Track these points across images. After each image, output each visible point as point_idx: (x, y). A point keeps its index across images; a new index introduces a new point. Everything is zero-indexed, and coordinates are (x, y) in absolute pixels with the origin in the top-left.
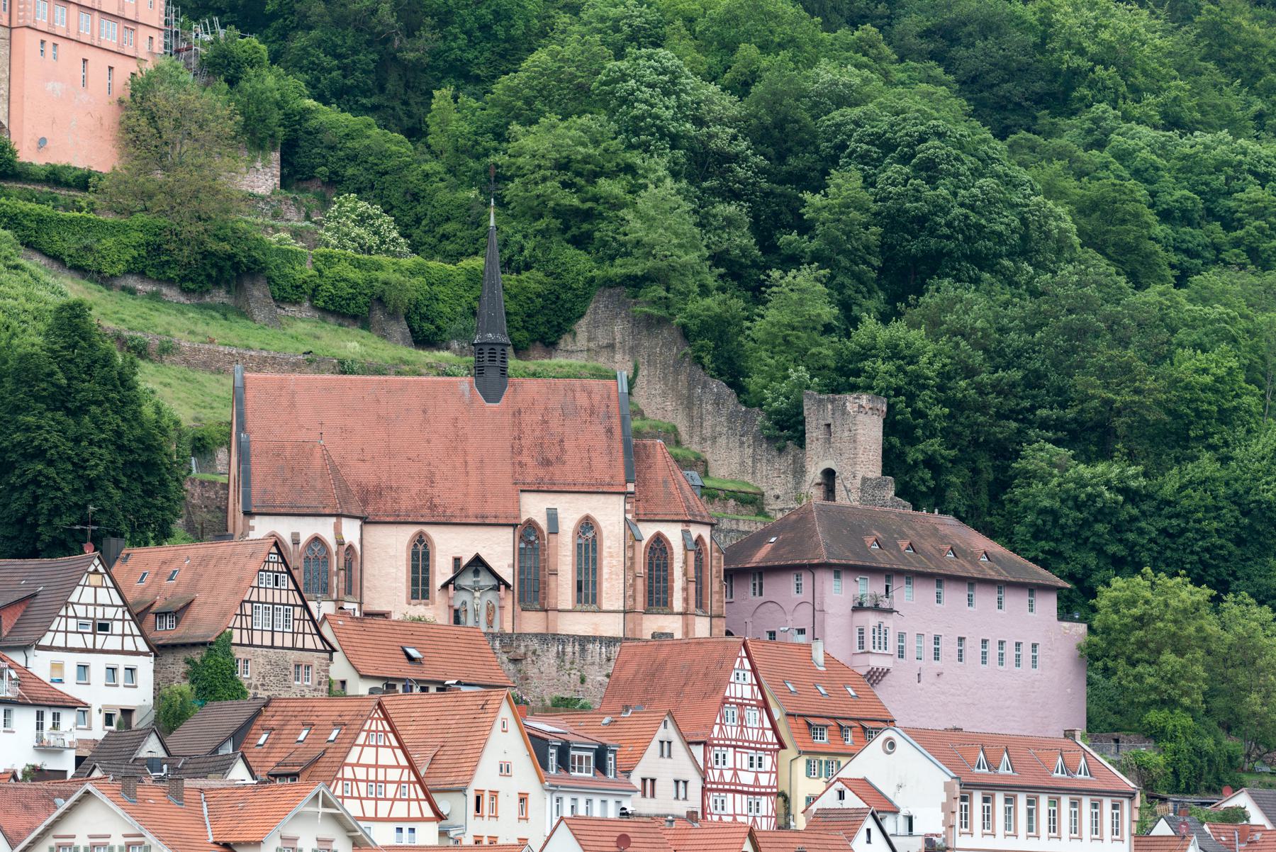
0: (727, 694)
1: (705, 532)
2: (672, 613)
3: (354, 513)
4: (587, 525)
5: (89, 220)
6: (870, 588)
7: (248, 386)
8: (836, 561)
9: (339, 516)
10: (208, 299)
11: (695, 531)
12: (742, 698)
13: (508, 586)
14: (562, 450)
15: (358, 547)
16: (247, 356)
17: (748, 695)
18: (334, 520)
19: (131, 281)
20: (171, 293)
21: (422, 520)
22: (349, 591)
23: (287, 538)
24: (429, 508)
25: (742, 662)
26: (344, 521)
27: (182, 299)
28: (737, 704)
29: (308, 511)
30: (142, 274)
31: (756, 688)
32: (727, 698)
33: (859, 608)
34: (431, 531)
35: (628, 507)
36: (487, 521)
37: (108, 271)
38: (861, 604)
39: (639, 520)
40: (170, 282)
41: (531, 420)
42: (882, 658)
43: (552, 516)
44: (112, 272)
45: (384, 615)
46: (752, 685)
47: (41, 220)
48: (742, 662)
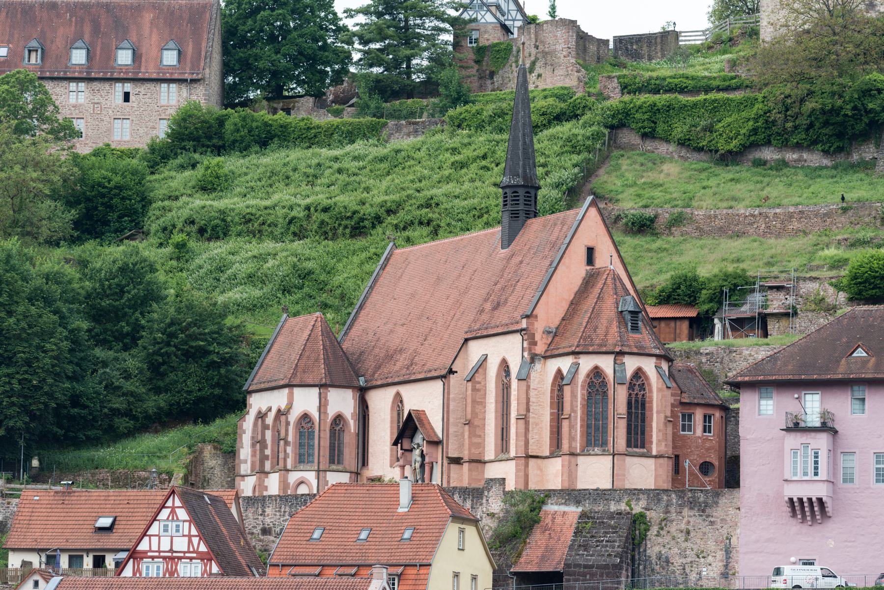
0: (139, 548)
1: (606, 364)
2: (648, 456)
3: (310, 381)
4: (505, 366)
5: (715, 100)
6: (813, 406)
7: (391, 262)
8: (747, 379)
9: (290, 386)
10: (855, 157)
11: (587, 364)
12: (171, 551)
13: (436, 443)
14: (513, 292)
15: (315, 415)
16: (771, 215)
17: (181, 544)
18: (286, 391)
19: (768, 154)
20: (814, 159)
21: (396, 380)
22: (303, 459)
23: (264, 410)
24: (408, 369)
25: (173, 512)
26: (296, 390)
27: (826, 162)
28: (164, 558)
29: (273, 384)
30: (768, 143)
31: (195, 540)
32: (146, 552)
33: (796, 427)
34: (404, 390)
35: (525, 344)
36: (429, 375)
37: (723, 146)
38: (797, 424)
39: (546, 358)
40: (798, 146)
41: (516, 260)
42: (805, 485)
43: (484, 361)
44: (728, 148)
45: (379, 479)
46: (190, 536)
47: (653, 109)
48: (173, 512)
